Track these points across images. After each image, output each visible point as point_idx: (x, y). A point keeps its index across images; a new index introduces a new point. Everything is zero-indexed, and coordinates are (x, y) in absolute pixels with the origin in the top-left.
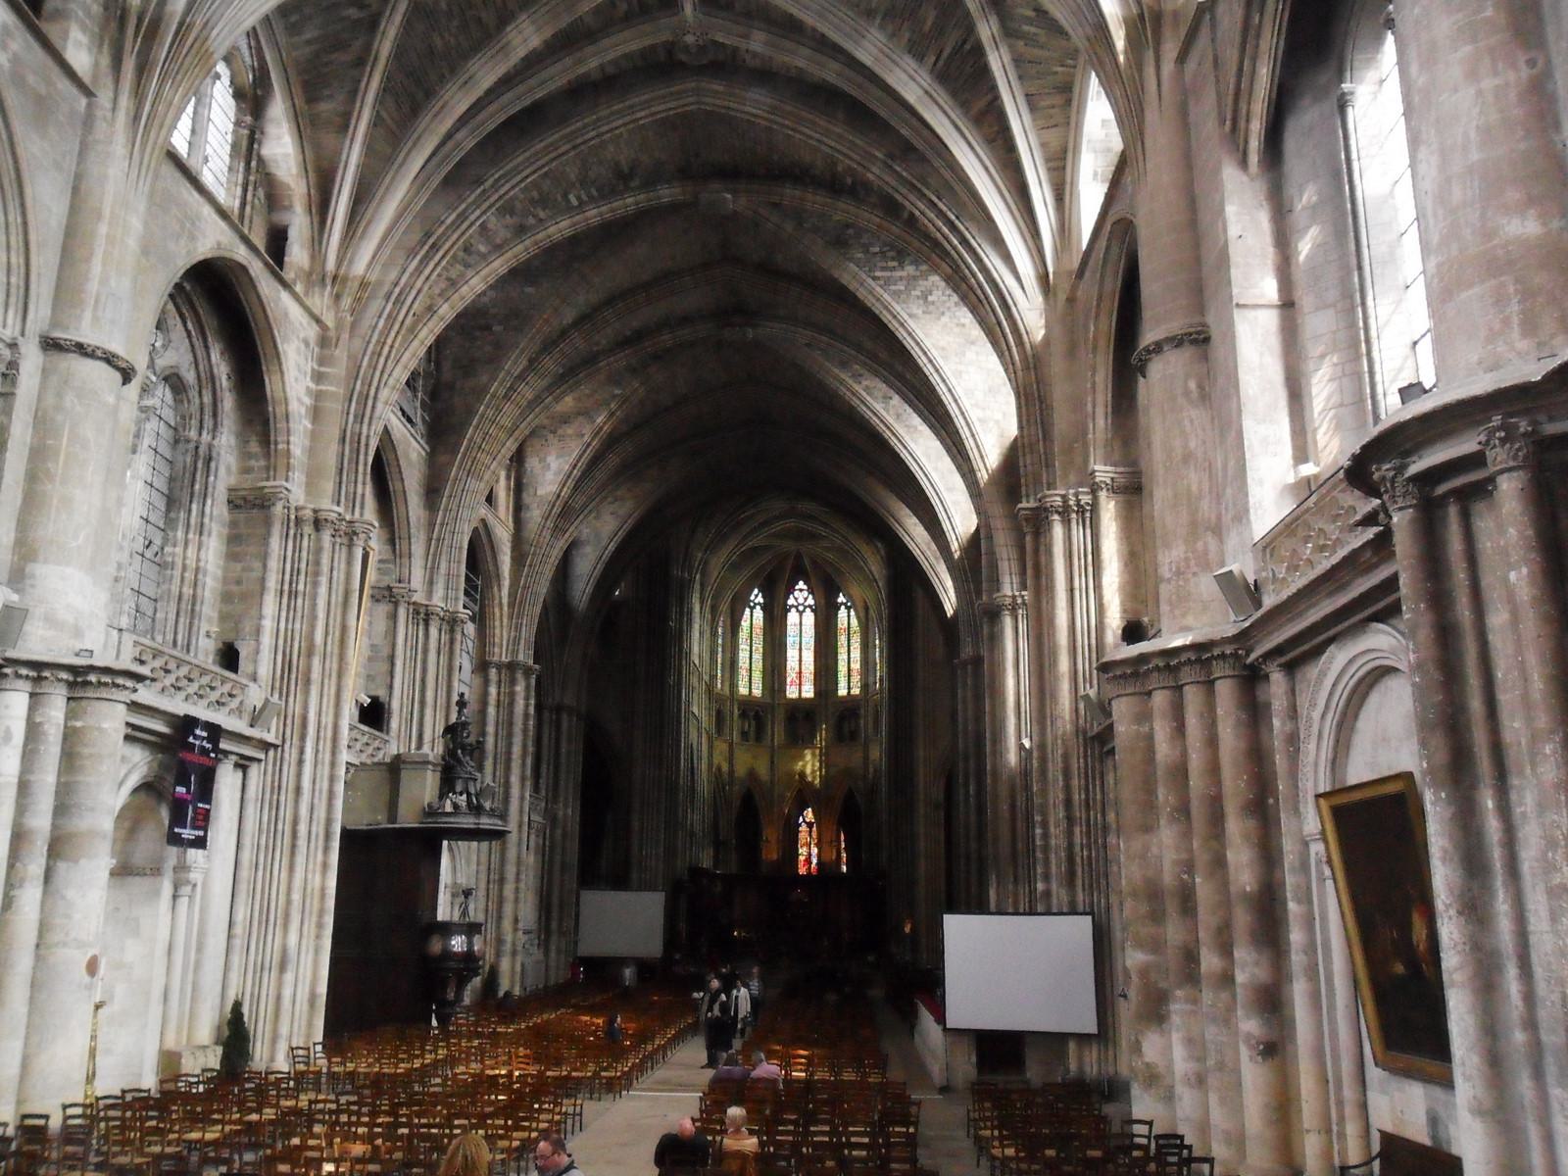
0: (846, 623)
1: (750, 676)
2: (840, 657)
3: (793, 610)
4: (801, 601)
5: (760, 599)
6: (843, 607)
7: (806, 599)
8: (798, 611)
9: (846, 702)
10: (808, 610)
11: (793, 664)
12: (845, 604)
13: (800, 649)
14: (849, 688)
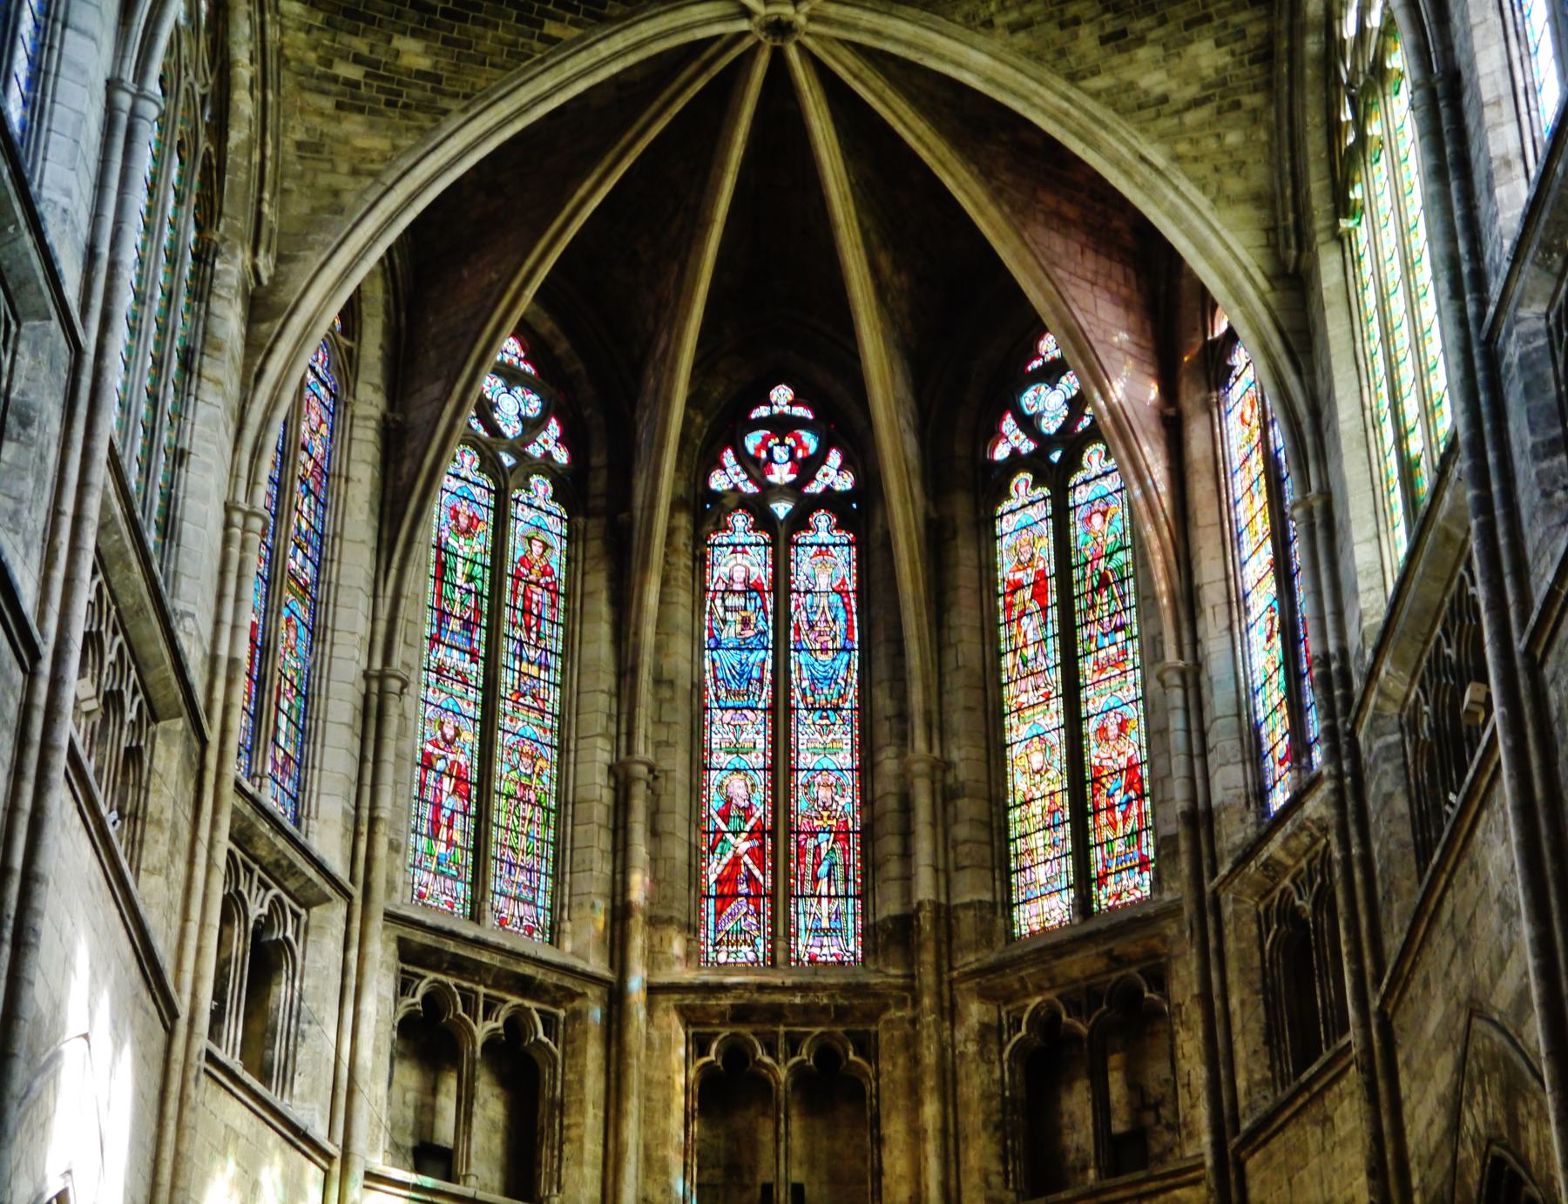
0: (1045, 548)
1: (482, 820)
2: (1017, 730)
3: (740, 520)
4: (781, 474)
5: (550, 443)
6: (1023, 478)
7: (807, 468)
8: (763, 520)
9: (1076, 966)
10: (822, 519)
11: (737, 787)
12: (1036, 465)
13: (780, 716)
14: (1084, 882)
